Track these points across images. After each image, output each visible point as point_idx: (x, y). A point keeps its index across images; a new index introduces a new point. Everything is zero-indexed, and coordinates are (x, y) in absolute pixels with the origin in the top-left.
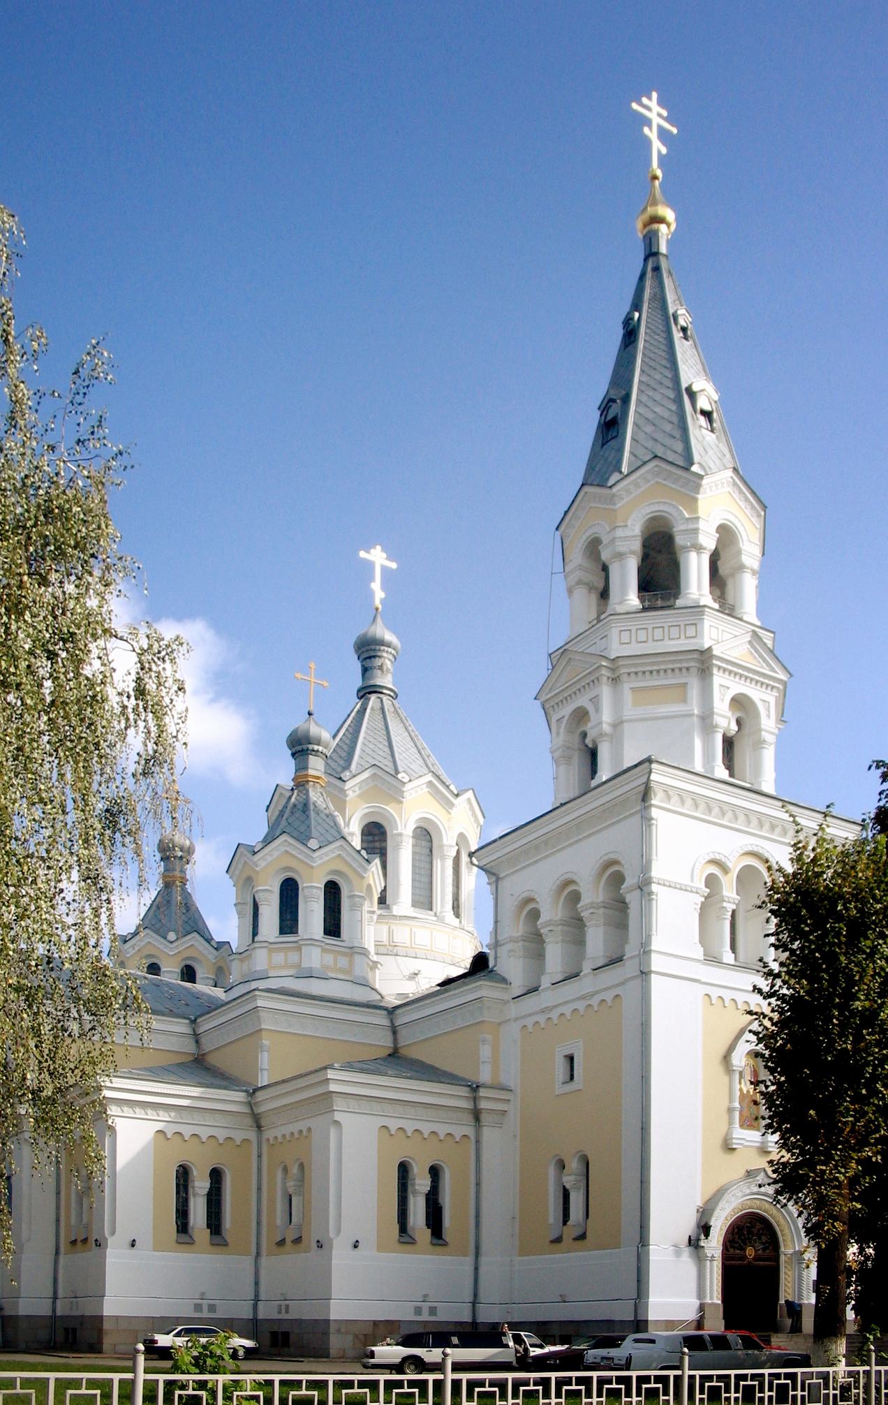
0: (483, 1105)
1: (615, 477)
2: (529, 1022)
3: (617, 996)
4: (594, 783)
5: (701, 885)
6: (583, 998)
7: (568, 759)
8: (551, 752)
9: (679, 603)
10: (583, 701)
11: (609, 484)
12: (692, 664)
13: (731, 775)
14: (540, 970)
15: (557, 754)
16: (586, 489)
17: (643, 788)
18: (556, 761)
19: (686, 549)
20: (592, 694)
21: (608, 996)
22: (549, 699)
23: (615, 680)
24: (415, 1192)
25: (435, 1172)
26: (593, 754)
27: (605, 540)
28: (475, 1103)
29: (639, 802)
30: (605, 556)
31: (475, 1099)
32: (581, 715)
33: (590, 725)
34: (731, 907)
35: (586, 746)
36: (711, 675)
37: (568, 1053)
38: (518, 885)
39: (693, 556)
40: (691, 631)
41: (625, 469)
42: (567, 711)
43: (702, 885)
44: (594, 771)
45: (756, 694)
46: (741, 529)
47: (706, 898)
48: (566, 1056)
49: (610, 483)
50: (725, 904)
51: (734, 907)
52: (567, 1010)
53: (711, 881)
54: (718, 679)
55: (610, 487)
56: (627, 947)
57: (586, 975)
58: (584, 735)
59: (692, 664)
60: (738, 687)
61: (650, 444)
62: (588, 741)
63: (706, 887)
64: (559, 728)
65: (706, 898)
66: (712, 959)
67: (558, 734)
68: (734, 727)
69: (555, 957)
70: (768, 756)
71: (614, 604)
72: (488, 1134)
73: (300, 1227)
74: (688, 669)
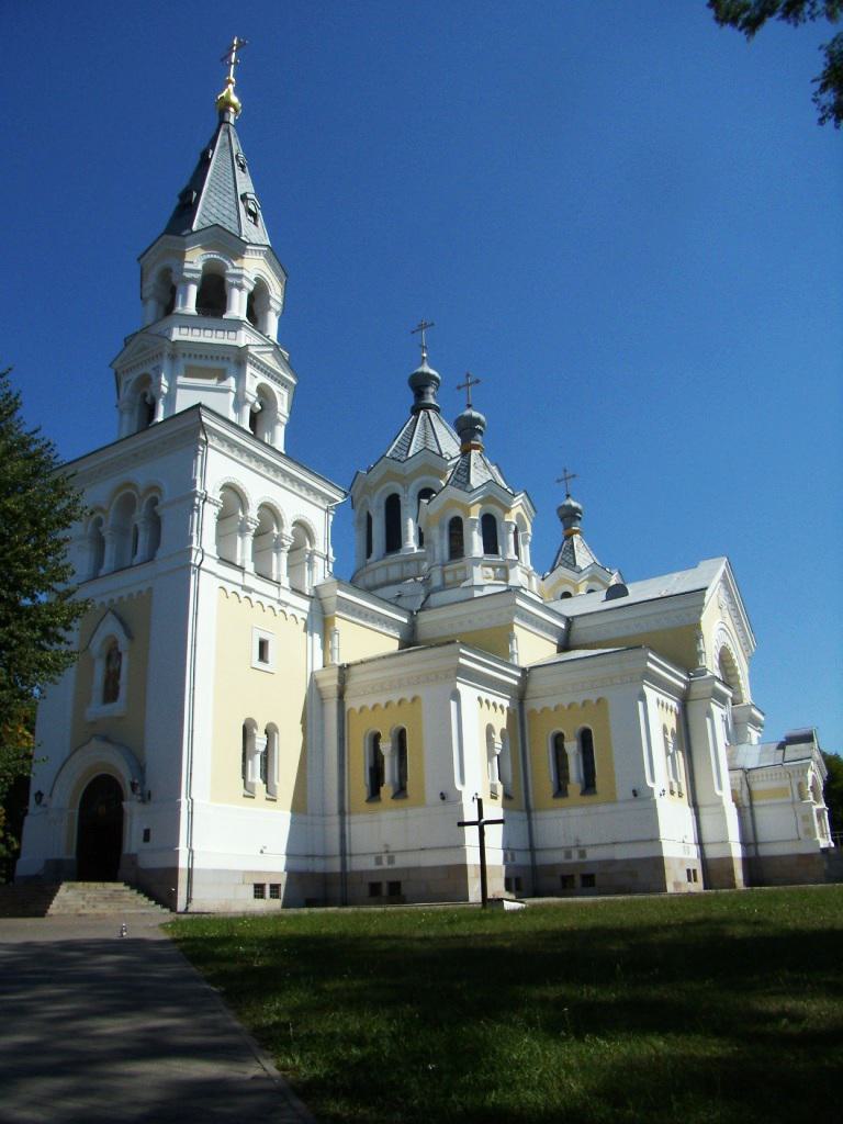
1: (187, 231)
9: (224, 317)
10: (148, 369)
11: (184, 234)
14: (99, 562)
16: (165, 237)
19: (232, 285)
23: (173, 357)
27: (175, 270)
30: (174, 279)
36: (245, 368)
39: (235, 292)
40: (232, 334)
41: (194, 228)
42: (134, 376)
45: (275, 387)
46: (271, 284)
49: (184, 234)
54: (250, 369)
55: (185, 236)
58: (145, 395)
60: (263, 379)
61: (212, 218)
62: (148, 399)
68: (258, 406)
70: (280, 431)
71: (179, 309)
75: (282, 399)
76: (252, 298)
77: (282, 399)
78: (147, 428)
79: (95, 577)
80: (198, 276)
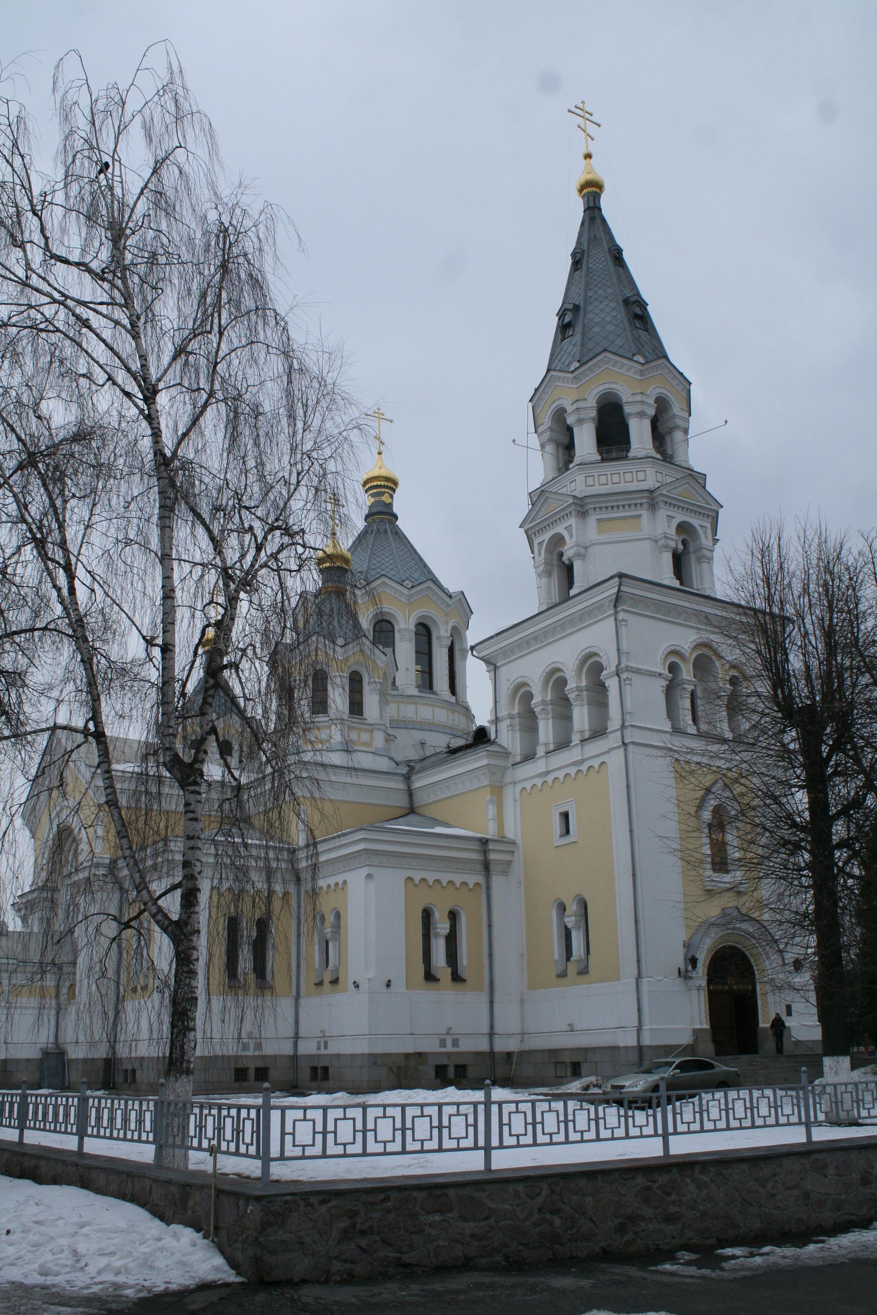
0: (492, 856)
2: (528, 785)
3: (603, 763)
4: (572, 592)
5: (666, 672)
6: (574, 764)
7: (549, 574)
8: (535, 568)
10: (560, 529)
12: (644, 501)
13: (681, 584)
14: (534, 742)
15: (541, 569)
17: (614, 597)
18: (539, 575)
20: (567, 524)
21: (596, 763)
22: (531, 528)
24: (437, 935)
25: (453, 916)
26: (569, 569)
28: (485, 854)
29: (612, 607)
31: (485, 852)
32: (559, 540)
33: (566, 548)
34: (690, 688)
35: (564, 563)
37: (563, 810)
38: (512, 672)
42: (546, 536)
43: (666, 672)
44: (570, 583)
47: (670, 681)
48: (561, 814)
50: (686, 686)
51: (693, 688)
52: (561, 774)
53: (673, 668)
56: (609, 723)
57: (576, 746)
58: (561, 554)
59: (644, 501)
62: (565, 559)
63: (670, 672)
64: (540, 550)
65: (670, 681)
66: (677, 731)
67: (540, 554)
68: (681, 547)
69: (546, 730)
72: (497, 881)
73: (337, 970)
74: (641, 504)
75: (705, 533)
76: (655, 423)
77: (705, 533)
78: (570, 598)
79: (529, 757)
80: (594, 413)
